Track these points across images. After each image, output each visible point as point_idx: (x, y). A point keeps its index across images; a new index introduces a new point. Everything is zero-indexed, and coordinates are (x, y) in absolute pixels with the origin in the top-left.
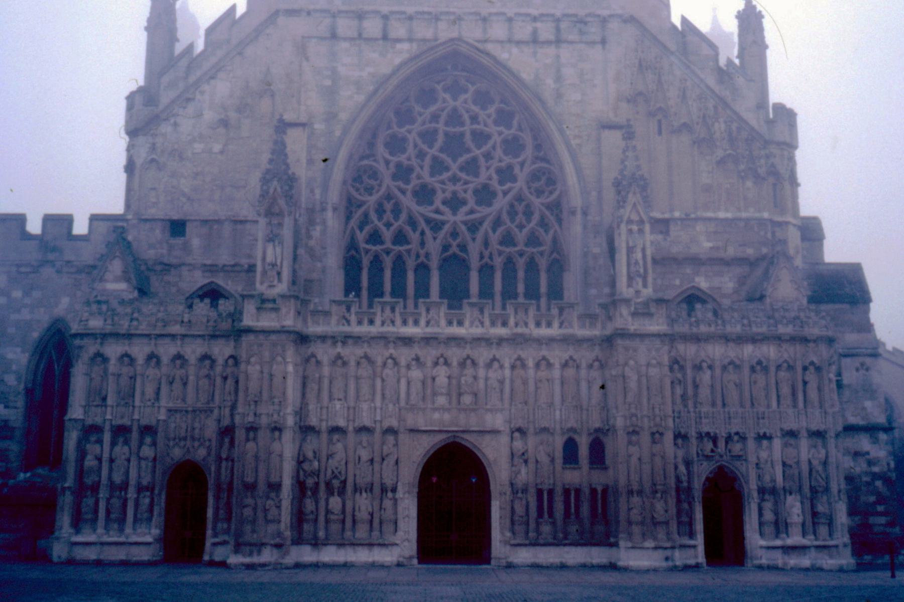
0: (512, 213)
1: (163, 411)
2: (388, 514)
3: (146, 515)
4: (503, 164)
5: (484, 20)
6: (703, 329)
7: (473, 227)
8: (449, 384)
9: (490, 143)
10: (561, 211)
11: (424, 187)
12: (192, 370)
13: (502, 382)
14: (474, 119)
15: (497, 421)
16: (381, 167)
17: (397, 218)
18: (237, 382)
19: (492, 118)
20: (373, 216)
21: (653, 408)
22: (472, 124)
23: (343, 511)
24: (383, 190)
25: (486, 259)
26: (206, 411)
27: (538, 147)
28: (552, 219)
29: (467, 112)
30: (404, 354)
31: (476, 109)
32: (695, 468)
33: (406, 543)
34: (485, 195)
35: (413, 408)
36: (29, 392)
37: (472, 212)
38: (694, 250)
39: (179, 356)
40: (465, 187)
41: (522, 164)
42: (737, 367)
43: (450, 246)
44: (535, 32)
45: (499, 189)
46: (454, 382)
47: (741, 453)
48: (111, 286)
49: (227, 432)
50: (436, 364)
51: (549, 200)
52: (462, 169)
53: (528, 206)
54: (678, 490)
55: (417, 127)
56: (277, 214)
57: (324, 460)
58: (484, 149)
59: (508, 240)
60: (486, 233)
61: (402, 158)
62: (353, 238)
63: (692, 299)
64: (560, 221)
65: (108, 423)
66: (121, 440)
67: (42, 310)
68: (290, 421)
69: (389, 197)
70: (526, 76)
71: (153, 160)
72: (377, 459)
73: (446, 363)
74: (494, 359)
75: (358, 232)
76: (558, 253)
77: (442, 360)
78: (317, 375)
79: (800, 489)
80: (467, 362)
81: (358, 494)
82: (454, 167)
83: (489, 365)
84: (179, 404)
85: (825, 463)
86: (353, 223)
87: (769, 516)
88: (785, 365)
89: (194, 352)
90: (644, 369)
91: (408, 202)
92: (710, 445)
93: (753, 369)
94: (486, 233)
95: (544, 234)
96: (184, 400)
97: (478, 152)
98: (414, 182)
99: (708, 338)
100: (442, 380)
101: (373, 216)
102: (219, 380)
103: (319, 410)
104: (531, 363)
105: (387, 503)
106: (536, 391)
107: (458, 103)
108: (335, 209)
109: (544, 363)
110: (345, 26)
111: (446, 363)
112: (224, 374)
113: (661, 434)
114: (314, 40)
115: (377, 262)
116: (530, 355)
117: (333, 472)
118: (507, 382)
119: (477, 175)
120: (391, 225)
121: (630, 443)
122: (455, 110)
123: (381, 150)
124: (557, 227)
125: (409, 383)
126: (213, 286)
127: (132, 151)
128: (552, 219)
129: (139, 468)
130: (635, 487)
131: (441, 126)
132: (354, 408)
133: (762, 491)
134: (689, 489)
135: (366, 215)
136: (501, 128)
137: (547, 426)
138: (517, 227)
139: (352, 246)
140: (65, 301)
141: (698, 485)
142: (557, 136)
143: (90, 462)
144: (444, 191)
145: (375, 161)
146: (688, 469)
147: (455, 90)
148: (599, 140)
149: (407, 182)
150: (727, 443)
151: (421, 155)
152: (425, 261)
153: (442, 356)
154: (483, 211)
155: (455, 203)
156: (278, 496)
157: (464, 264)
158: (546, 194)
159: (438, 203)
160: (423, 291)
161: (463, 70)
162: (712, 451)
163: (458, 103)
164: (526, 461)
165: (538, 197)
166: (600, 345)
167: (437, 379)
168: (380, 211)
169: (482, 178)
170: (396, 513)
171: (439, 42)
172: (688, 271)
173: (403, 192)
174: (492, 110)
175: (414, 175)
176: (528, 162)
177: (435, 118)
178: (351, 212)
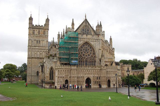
6: (108, 68)
15: (92, 76)
30: (84, 70)
34: (89, 55)
35: (85, 75)
48: (58, 64)
59: (91, 59)
63: (106, 65)
69: (81, 55)
70: (93, 44)
80: (89, 71)
91: (82, 56)
99: (108, 69)
105: (83, 83)
116: (95, 70)
142: (95, 50)
151: (83, 51)
154: (89, 57)
155: (86, 56)
169: (89, 54)
177: (84, 48)
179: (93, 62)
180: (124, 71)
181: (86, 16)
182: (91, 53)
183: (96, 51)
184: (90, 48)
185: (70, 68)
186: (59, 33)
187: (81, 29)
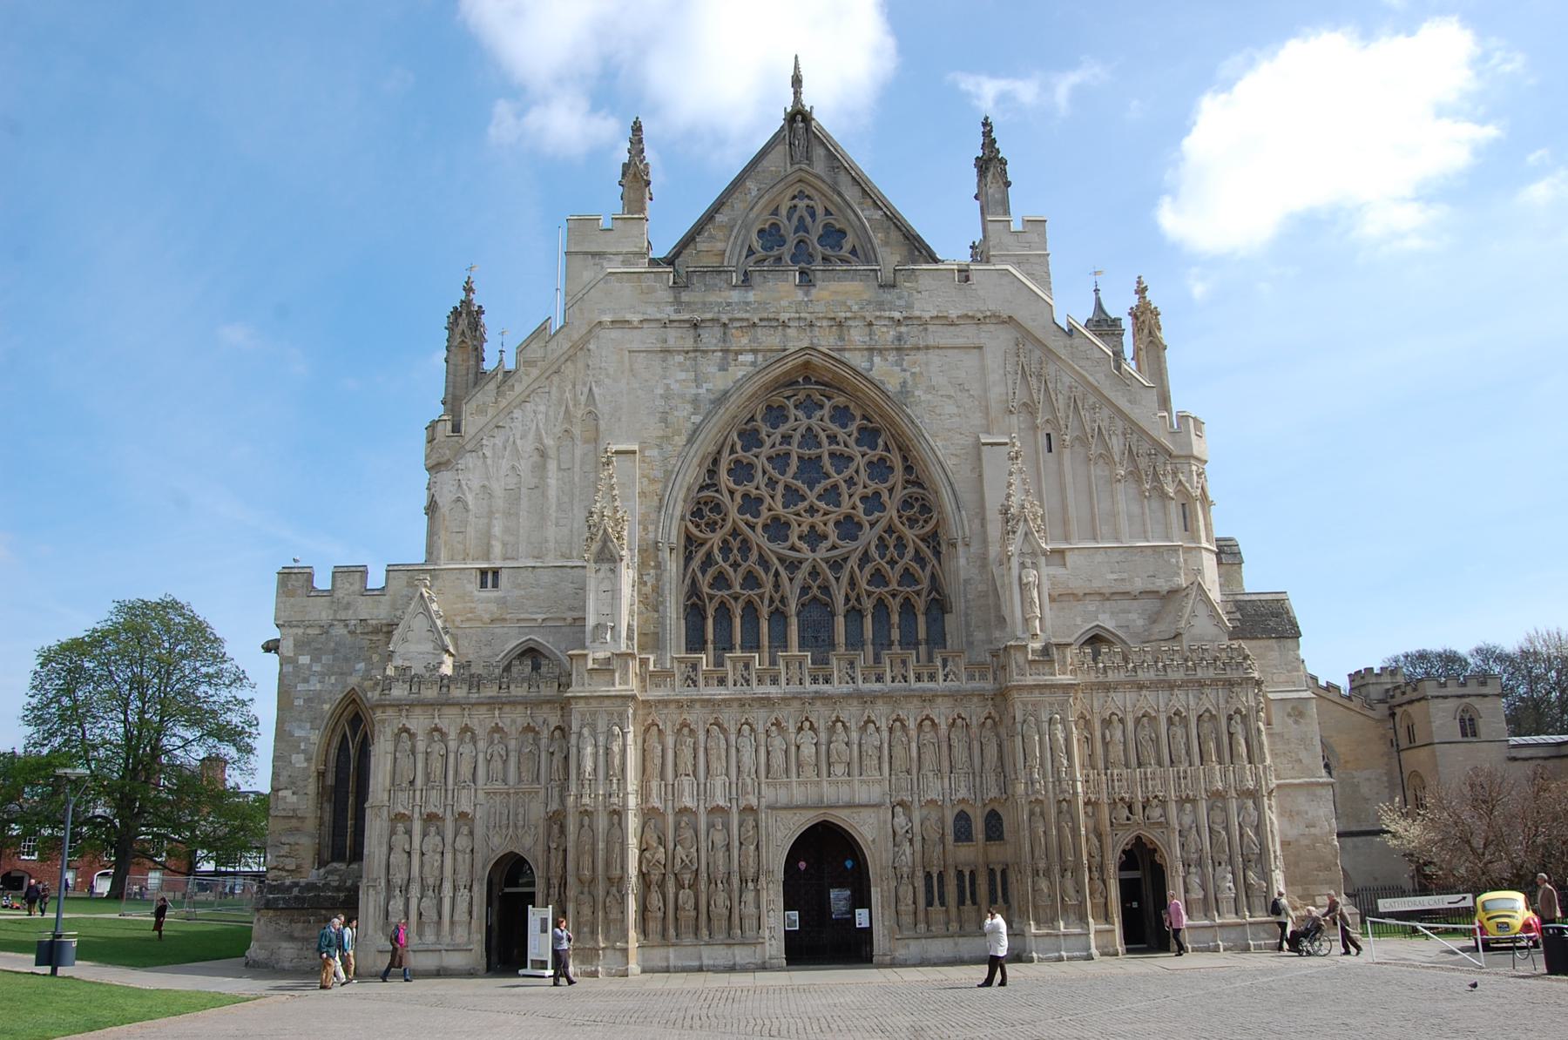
0: (882, 545)
1: (481, 794)
2: (750, 910)
3: (466, 917)
4: (869, 491)
5: (840, 325)
6: (1112, 676)
7: (836, 565)
8: (817, 753)
9: (853, 466)
10: (939, 544)
11: (776, 519)
12: (513, 744)
13: (880, 748)
14: (833, 439)
15: (875, 793)
16: (726, 498)
17: (745, 559)
18: (566, 758)
19: (853, 437)
20: (719, 557)
21: (1059, 773)
22: (830, 444)
23: (696, 908)
24: (729, 525)
25: (853, 602)
26: (530, 793)
27: (908, 469)
28: (928, 553)
29: (824, 431)
31: (835, 428)
32: (1108, 841)
33: (773, 941)
36: (321, 775)
37: (834, 547)
38: (1097, 584)
39: (497, 729)
40: (825, 518)
41: (891, 490)
42: (1153, 719)
43: (810, 588)
44: (899, 338)
45: (865, 519)
46: (824, 748)
47: (1162, 819)
48: (413, 648)
49: (557, 821)
50: (801, 729)
51: (928, 528)
52: (820, 497)
53: (900, 538)
55: (766, 451)
56: (608, 560)
57: (671, 846)
58: (847, 473)
60: (852, 573)
61: (750, 487)
62: (694, 582)
64: (937, 554)
65: (417, 809)
66: (433, 829)
67: (333, 679)
68: (632, 801)
69: (735, 533)
70: (892, 386)
71: (458, 499)
72: (737, 843)
73: (812, 727)
74: (869, 721)
75: (699, 575)
76: (939, 594)
77: (807, 724)
78: (660, 748)
79: (1231, 861)
81: (713, 885)
82: (812, 497)
83: (863, 729)
84: (499, 785)
85: (1259, 828)
86: (696, 564)
87: (1197, 894)
88: (1207, 714)
89: (513, 722)
90: (1046, 726)
91: (759, 538)
92: (1126, 812)
93: (1170, 719)
94: (852, 573)
95: (920, 571)
96: (505, 781)
97: (836, 478)
98: (765, 514)
100: (808, 751)
101: (719, 557)
102: (543, 755)
103: (663, 786)
104: (912, 724)
105: (749, 896)
106: (919, 757)
107: (814, 422)
108: (671, 550)
109: (927, 722)
110: (674, 337)
111: (812, 727)
112: (551, 750)
113: (1069, 802)
114: (645, 354)
115: (723, 612)
117: (682, 861)
118: (886, 746)
119: (838, 505)
120: (740, 565)
121: (1032, 813)
122: (809, 429)
123: (724, 478)
124: (935, 562)
125: (768, 753)
126: (532, 645)
127: (433, 490)
128: (928, 553)
129: (455, 859)
130: (1042, 865)
131: (794, 449)
132: (705, 784)
133: (1187, 865)
134: (1102, 868)
135: (709, 555)
136: (865, 449)
137: (935, 797)
138: (888, 563)
139: (694, 590)
140: (361, 666)
143: (398, 858)
144: (799, 525)
145: (717, 491)
146: (1100, 841)
147: (810, 406)
148: (980, 459)
149: (757, 515)
150: (1144, 808)
151: (772, 483)
152: (780, 605)
153: (807, 719)
154: (848, 546)
155: (814, 537)
156: (619, 891)
158: (921, 523)
159: (794, 538)
160: (779, 640)
161: (817, 383)
162: (1128, 819)
163: (814, 422)
164: (911, 841)
165: (911, 527)
166: (992, 699)
167: (802, 748)
168: (725, 549)
169: (845, 508)
170: (758, 907)
171: (787, 353)
172: (1091, 608)
173: (753, 527)
174: (853, 427)
175: (764, 508)
176: (899, 486)
177: (786, 439)
178: (691, 552)
179: (907, 607)
180: (1423, 754)
181: (797, 81)
182: (873, 502)
183: (936, 472)
184: (869, 435)
185: (548, 691)
186: (469, 289)
187: (746, 226)
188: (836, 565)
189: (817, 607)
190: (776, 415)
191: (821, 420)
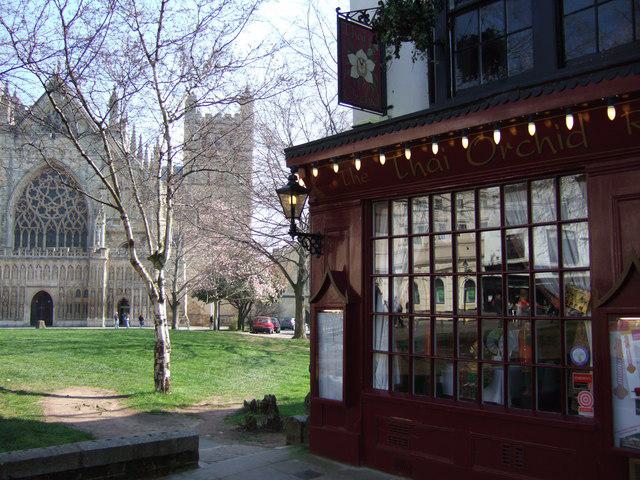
0: (71, 216)
7: (58, 221)
11: (42, 207)
15: (54, 283)
54: (108, 305)
59: (69, 225)
64: (86, 218)
91: (37, 213)
115: (25, 233)
123: (28, 195)
139: (17, 226)
141: (116, 303)
147: (54, 174)
151: (41, 197)
154: (61, 216)
157: (54, 233)
168: (27, 215)
188: (58, 221)
189: (51, 233)
190: (44, 176)
191: (56, 179)
